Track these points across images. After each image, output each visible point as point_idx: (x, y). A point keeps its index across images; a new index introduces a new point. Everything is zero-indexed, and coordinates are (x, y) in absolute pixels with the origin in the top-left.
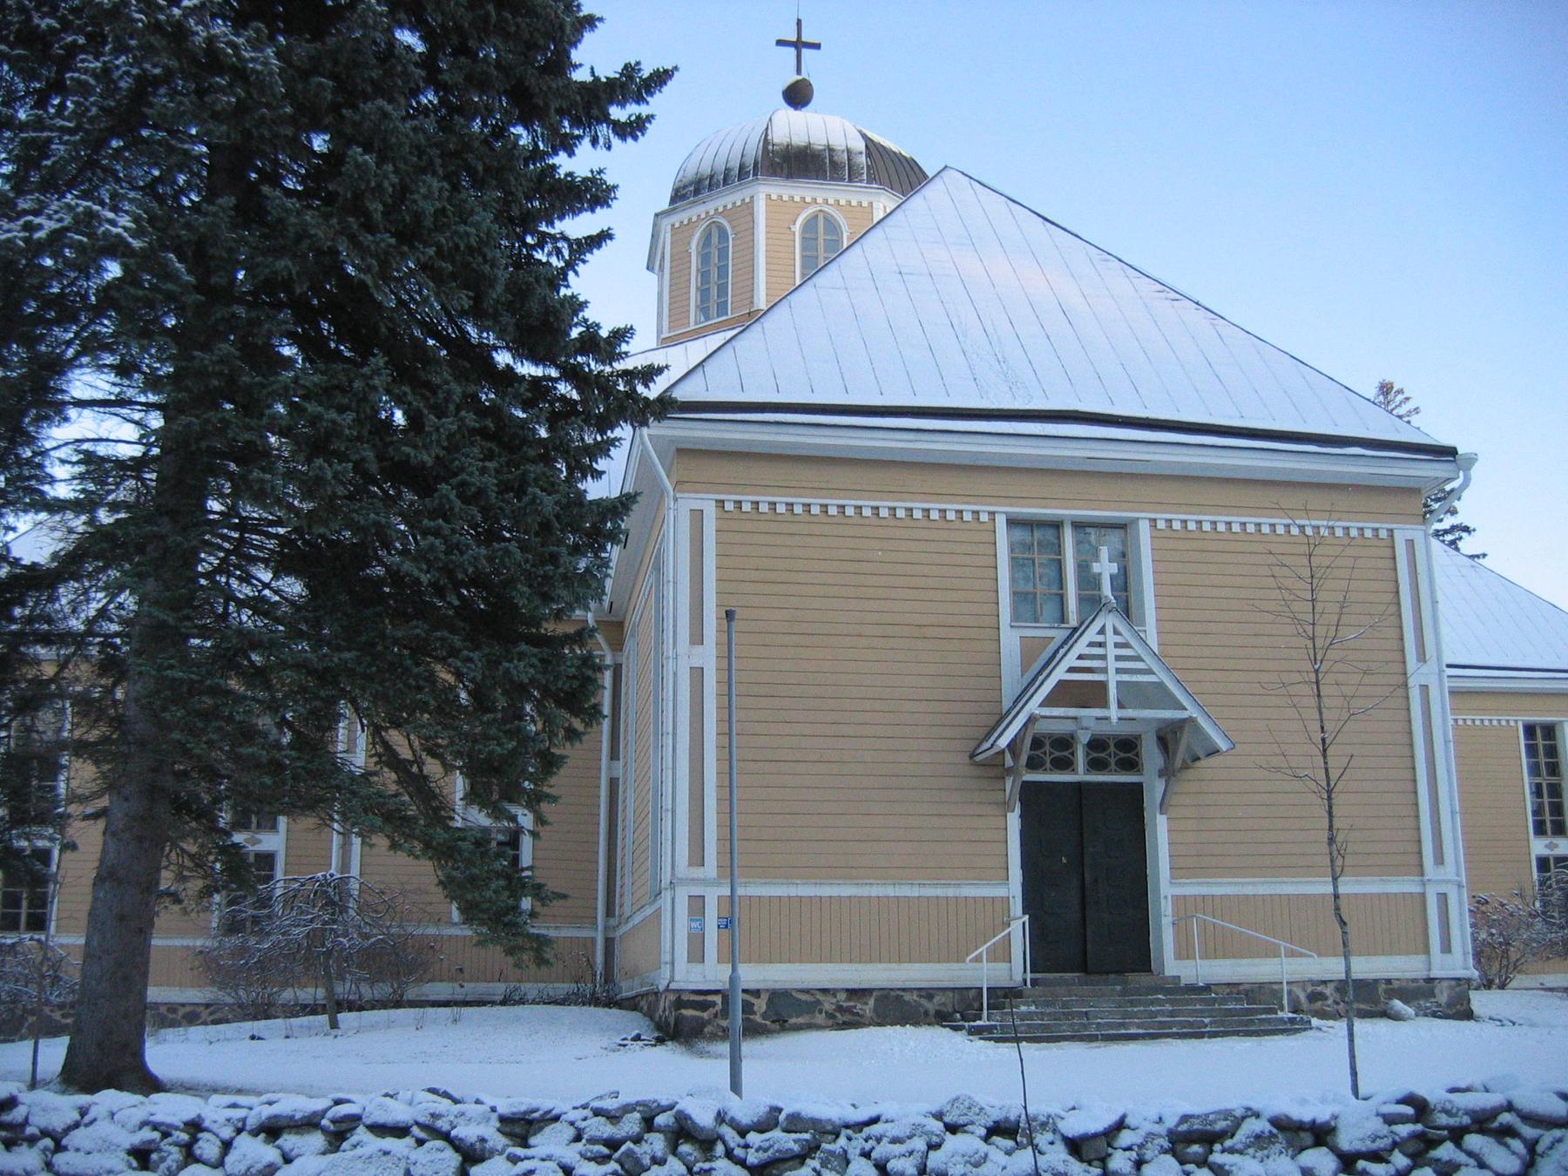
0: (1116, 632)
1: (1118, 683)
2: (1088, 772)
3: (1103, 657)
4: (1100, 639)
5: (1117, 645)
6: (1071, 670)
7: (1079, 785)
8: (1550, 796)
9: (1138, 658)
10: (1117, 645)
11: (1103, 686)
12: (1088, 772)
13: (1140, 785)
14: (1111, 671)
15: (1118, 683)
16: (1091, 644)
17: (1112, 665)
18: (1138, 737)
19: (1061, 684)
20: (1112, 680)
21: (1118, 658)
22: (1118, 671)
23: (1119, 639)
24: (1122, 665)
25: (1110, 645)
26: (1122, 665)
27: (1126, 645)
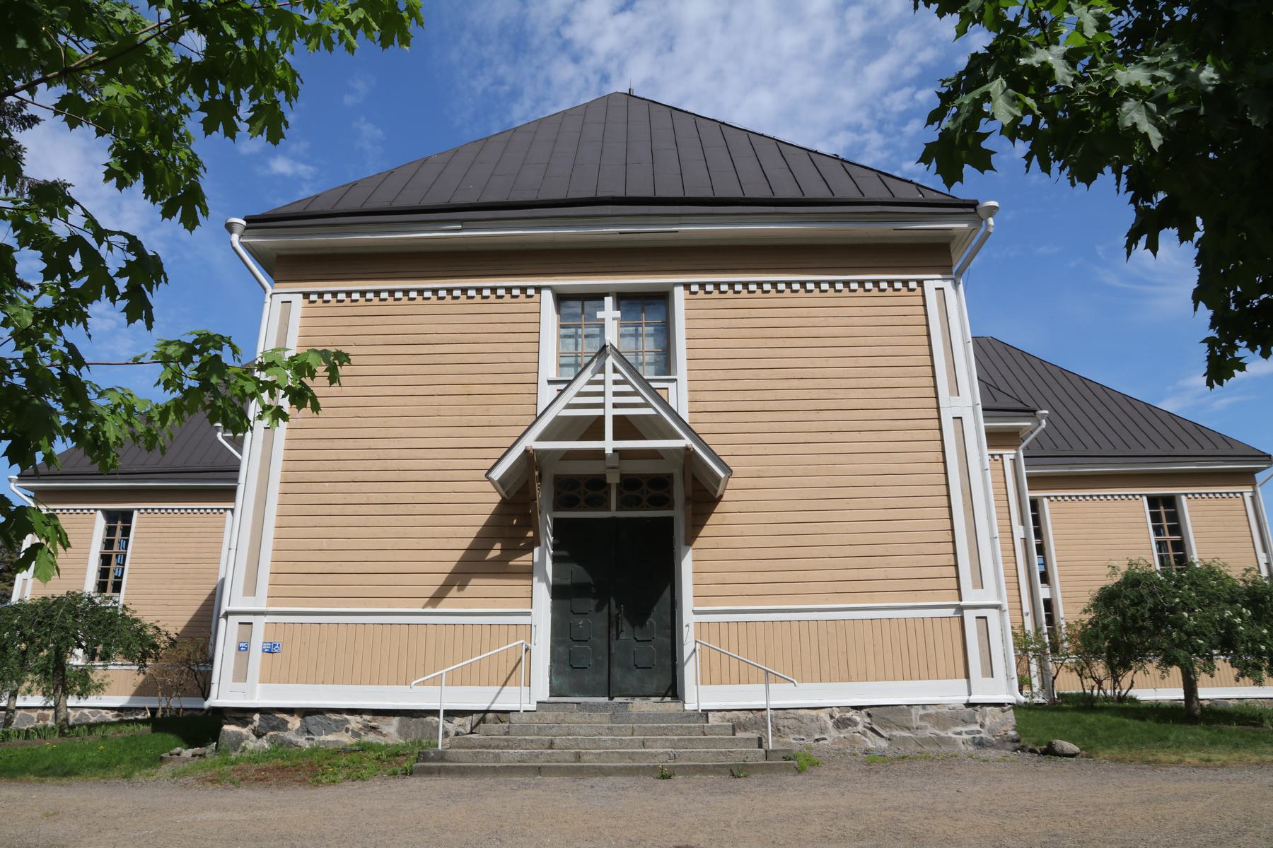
0: (615, 370)
1: (614, 417)
2: (619, 508)
3: (602, 394)
4: (599, 377)
5: (616, 382)
6: (569, 406)
7: (614, 519)
8: (1162, 527)
9: (636, 393)
10: (616, 382)
11: (601, 419)
12: (619, 508)
13: (671, 519)
14: (609, 406)
15: (614, 417)
16: (590, 383)
17: (610, 400)
18: (671, 476)
19: (558, 419)
20: (609, 413)
21: (616, 394)
22: (615, 406)
23: (618, 377)
24: (599, 400)
25: (609, 383)
26: (599, 400)
27: (625, 382)
